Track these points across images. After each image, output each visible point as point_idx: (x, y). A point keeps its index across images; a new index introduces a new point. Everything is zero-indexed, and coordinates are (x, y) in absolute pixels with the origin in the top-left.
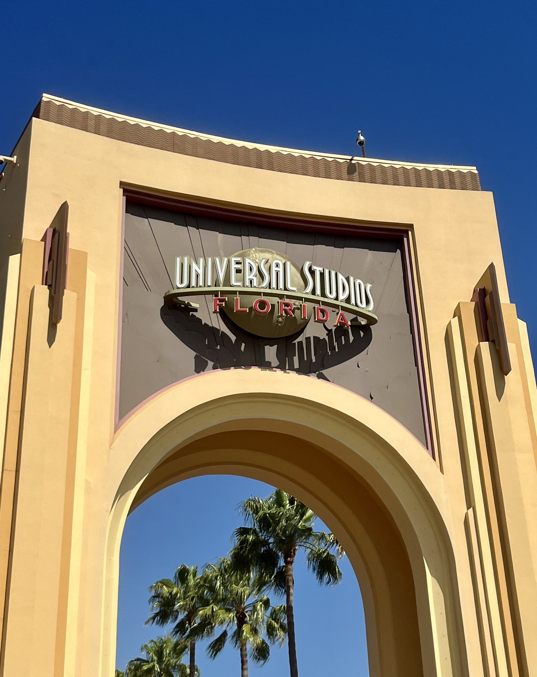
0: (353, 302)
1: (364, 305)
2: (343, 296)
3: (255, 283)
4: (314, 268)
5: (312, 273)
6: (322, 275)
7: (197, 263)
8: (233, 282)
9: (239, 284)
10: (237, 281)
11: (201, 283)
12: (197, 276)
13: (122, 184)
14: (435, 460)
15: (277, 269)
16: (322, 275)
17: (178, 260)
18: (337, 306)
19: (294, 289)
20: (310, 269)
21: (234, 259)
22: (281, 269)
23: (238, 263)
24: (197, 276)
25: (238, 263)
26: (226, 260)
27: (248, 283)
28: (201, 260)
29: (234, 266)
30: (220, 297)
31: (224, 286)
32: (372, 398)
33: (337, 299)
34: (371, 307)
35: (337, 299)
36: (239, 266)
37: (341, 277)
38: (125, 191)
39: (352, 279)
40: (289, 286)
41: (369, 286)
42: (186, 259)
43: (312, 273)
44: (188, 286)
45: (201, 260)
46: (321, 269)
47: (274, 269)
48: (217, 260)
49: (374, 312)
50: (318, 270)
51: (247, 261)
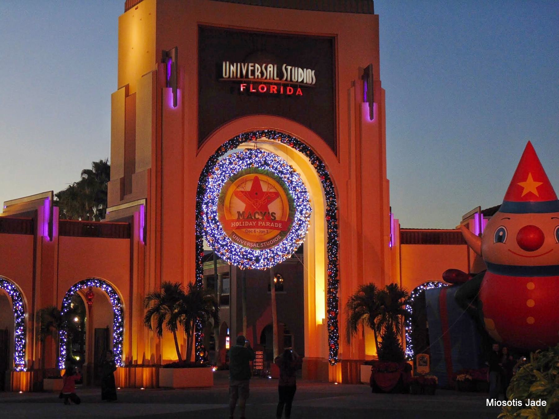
2: (300, 80)
6: (291, 70)
7: (233, 66)
8: (250, 76)
9: (252, 77)
10: (251, 75)
14: (336, 156)
20: (286, 67)
25: (252, 66)
28: (235, 64)
29: (250, 68)
31: (246, 78)
41: (313, 72)
43: (286, 70)
45: (235, 64)
50: (289, 68)
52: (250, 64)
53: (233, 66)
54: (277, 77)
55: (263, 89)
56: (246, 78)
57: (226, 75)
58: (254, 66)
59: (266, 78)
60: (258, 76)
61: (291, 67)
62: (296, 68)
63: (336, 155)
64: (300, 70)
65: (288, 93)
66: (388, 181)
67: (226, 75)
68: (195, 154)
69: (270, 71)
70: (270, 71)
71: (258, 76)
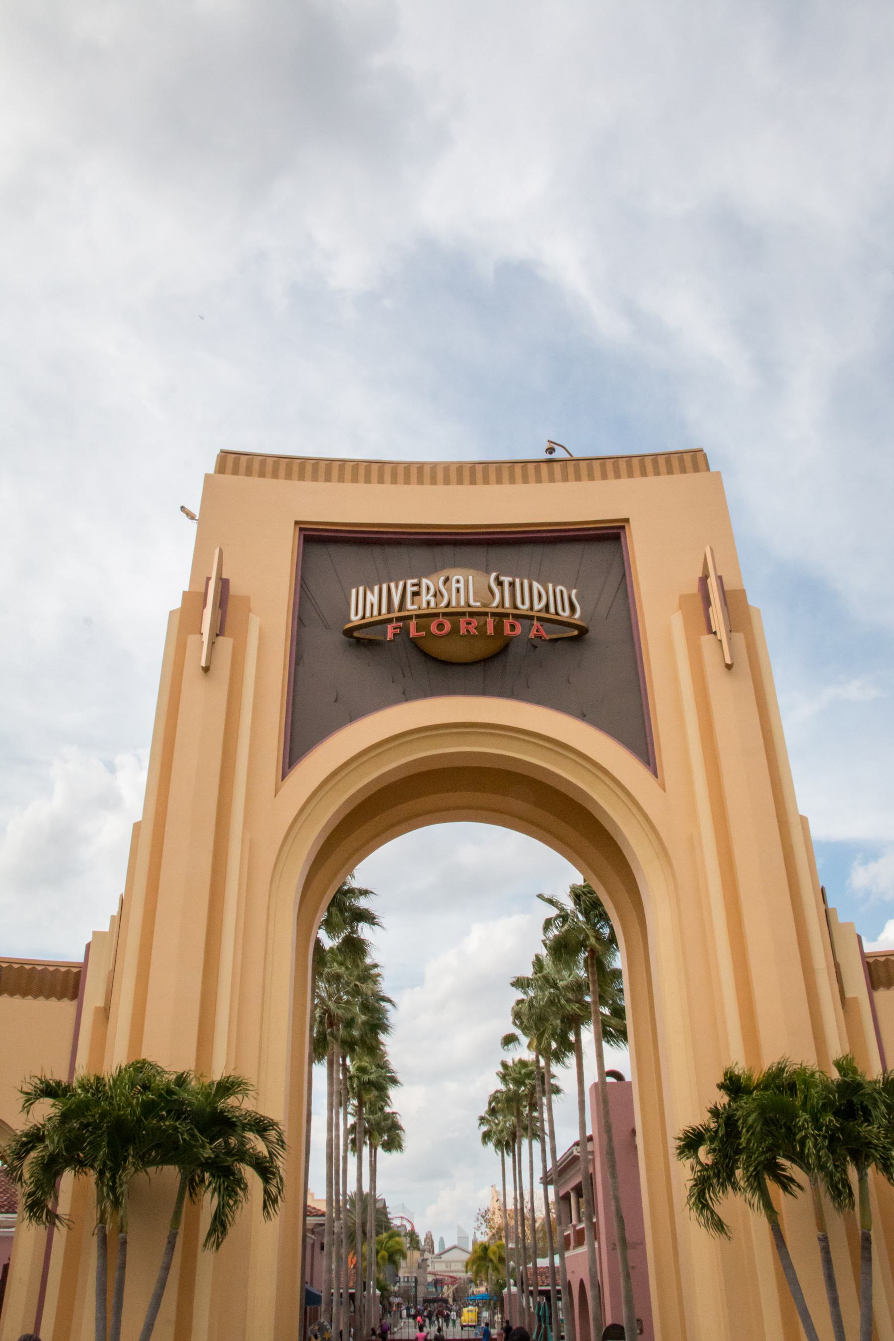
0: (552, 610)
1: (567, 613)
3: (432, 604)
4: (502, 578)
5: (500, 584)
6: (512, 584)
7: (372, 592)
8: (409, 606)
9: (415, 607)
10: (413, 603)
11: (375, 612)
12: (372, 605)
13: (297, 523)
15: (458, 585)
16: (512, 584)
17: (354, 591)
18: (531, 618)
19: (478, 604)
21: (409, 582)
22: (461, 585)
23: (414, 585)
24: (372, 605)
25: (414, 585)
26: (401, 584)
27: (424, 605)
28: (376, 588)
29: (410, 589)
30: (396, 621)
32: (585, 716)
33: (531, 608)
34: (577, 615)
35: (531, 608)
36: (415, 589)
37: (536, 585)
38: (301, 529)
39: (550, 586)
40: (472, 603)
41: (574, 592)
42: (361, 589)
43: (500, 584)
44: (364, 617)
45: (376, 588)
46: (510, 579)
47: (454, 585)
48: (393, 585)
49: (581, 618)
50: (506, 580)
51: (425, 581)
52: (409, 582)
53: (372, 592)
54: (475, 601)
55: (440, 626)
56: (400, 610)
57: (356, 614)
58: (418, 585)
59: (448, 605)
60: (428, 603)
61: (510, 579)
62: (526, 582)
63: (655, 774)
64: (536, 585)
65: (507, 631)
66: (804, 821)
67: (356, 614)
68: (273, 793)
69: (458, 590)
70: (458, 590)
71: (428, 603)
